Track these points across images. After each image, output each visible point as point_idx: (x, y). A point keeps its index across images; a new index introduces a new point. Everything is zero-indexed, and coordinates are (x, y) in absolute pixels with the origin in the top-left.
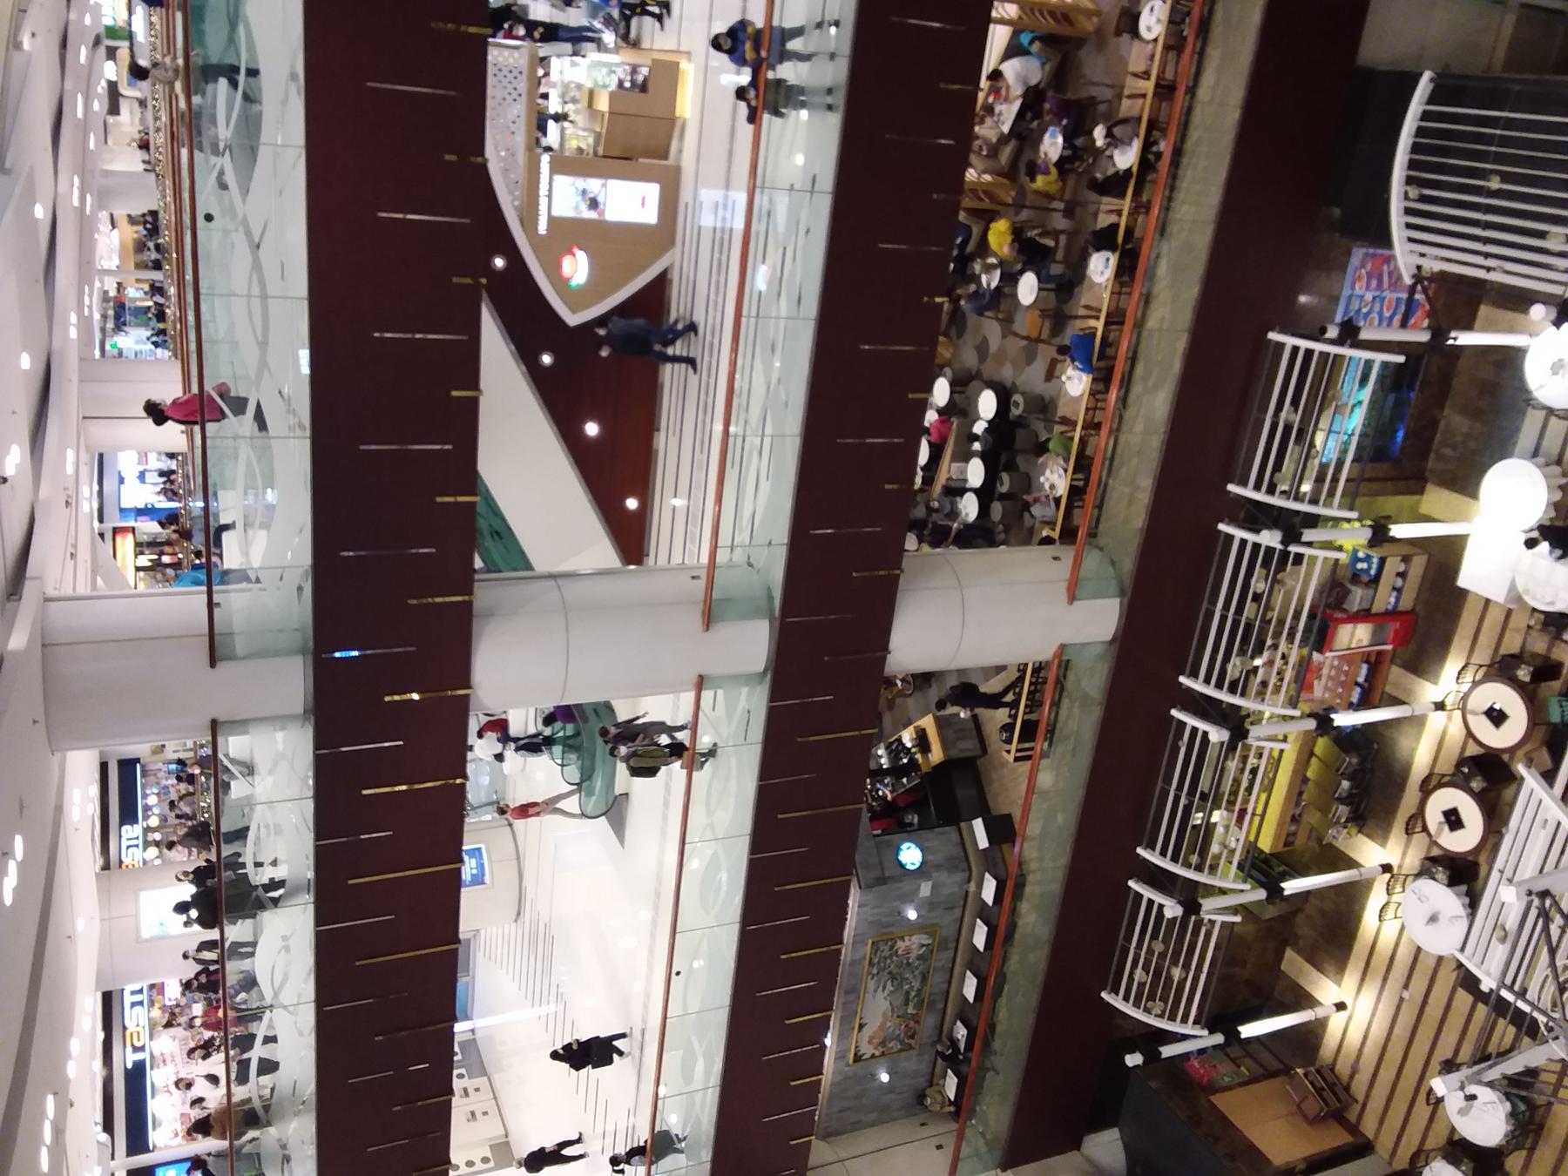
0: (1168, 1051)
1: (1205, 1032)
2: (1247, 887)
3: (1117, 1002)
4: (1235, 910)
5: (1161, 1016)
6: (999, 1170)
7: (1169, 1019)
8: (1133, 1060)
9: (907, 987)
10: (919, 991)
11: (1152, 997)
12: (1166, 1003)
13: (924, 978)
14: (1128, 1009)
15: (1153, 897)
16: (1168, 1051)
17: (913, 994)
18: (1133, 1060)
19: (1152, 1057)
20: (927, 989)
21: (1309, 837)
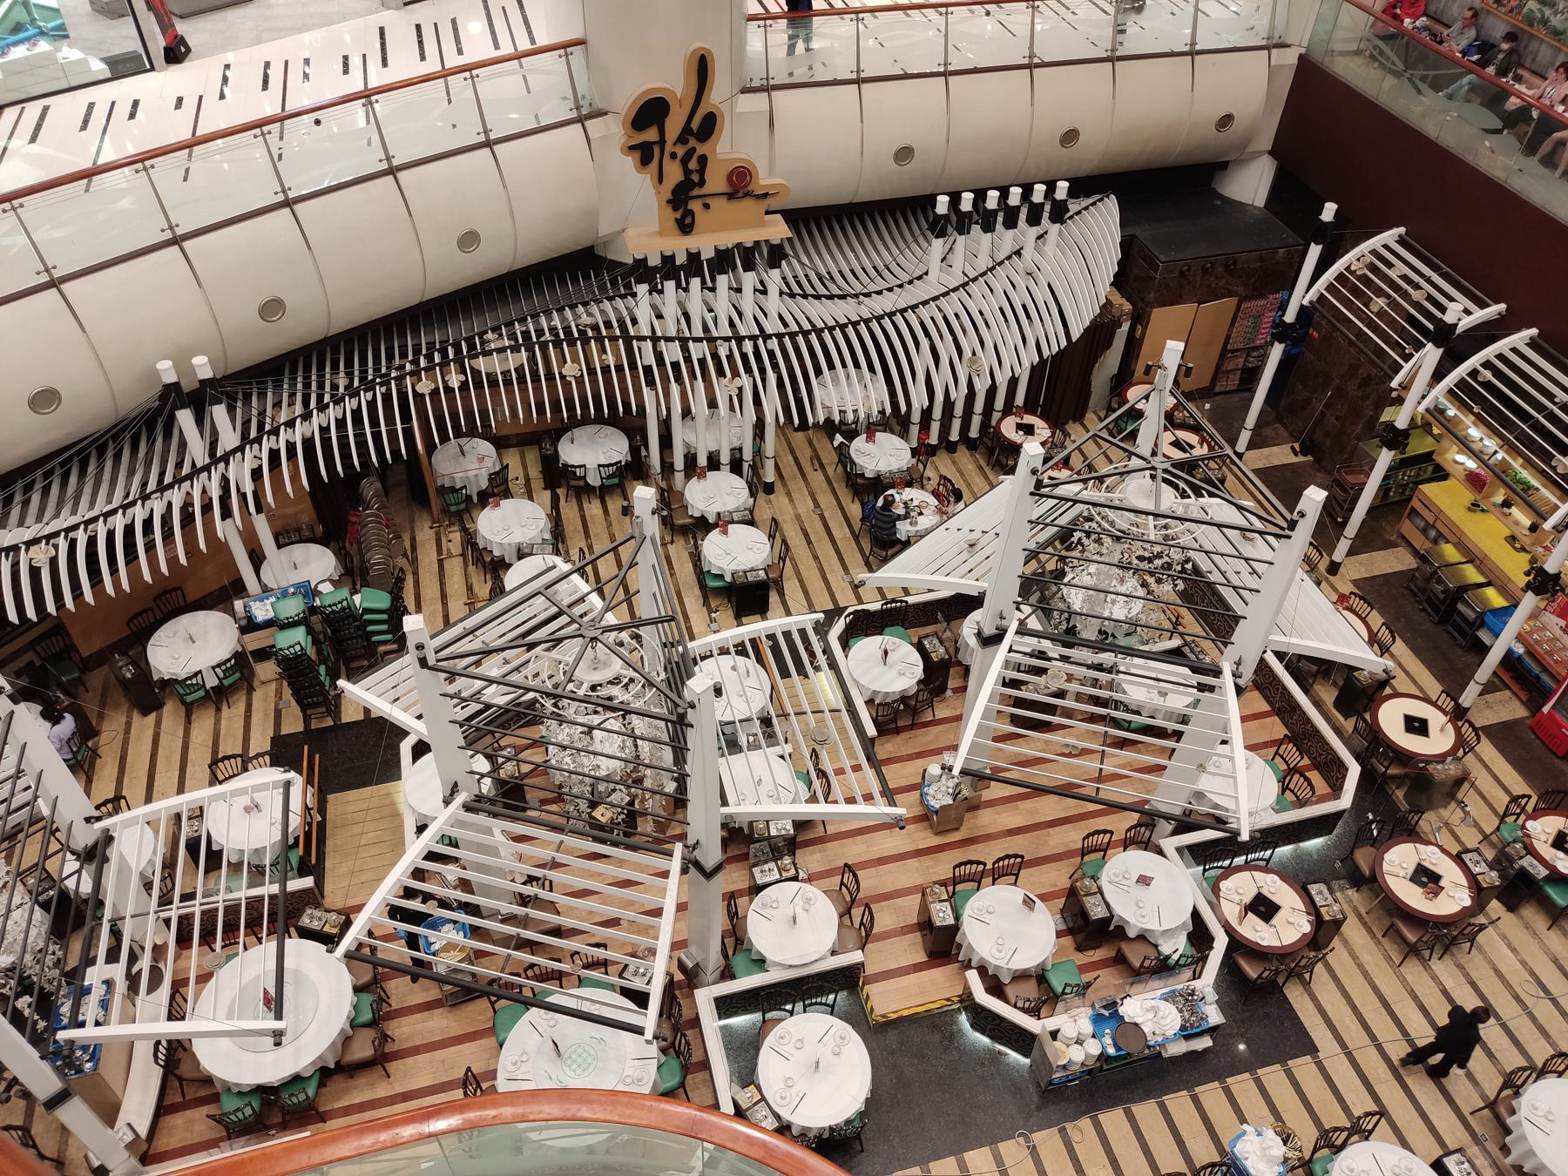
0: (1314, 251)
1: (1305, 302)
2: (1421, 409)
3: (1390, 236)
4: (1405, 387)
5: (1348, 269)
6: (1303, 51)
7: (1341, 274)
8: (1329, 212)
9: (1561, 7)
10: (1544, 22)
11: (1373, 268)
12: (1359, 278)
13: (1556, 33)
14: (1375, 242)
15: (1472, 318)
16: (1314, 251)
17: (1548, 12)
18: (1329, 212)
19: (1317, 231)
20: (1542, 32)
21: (1403, 537)
